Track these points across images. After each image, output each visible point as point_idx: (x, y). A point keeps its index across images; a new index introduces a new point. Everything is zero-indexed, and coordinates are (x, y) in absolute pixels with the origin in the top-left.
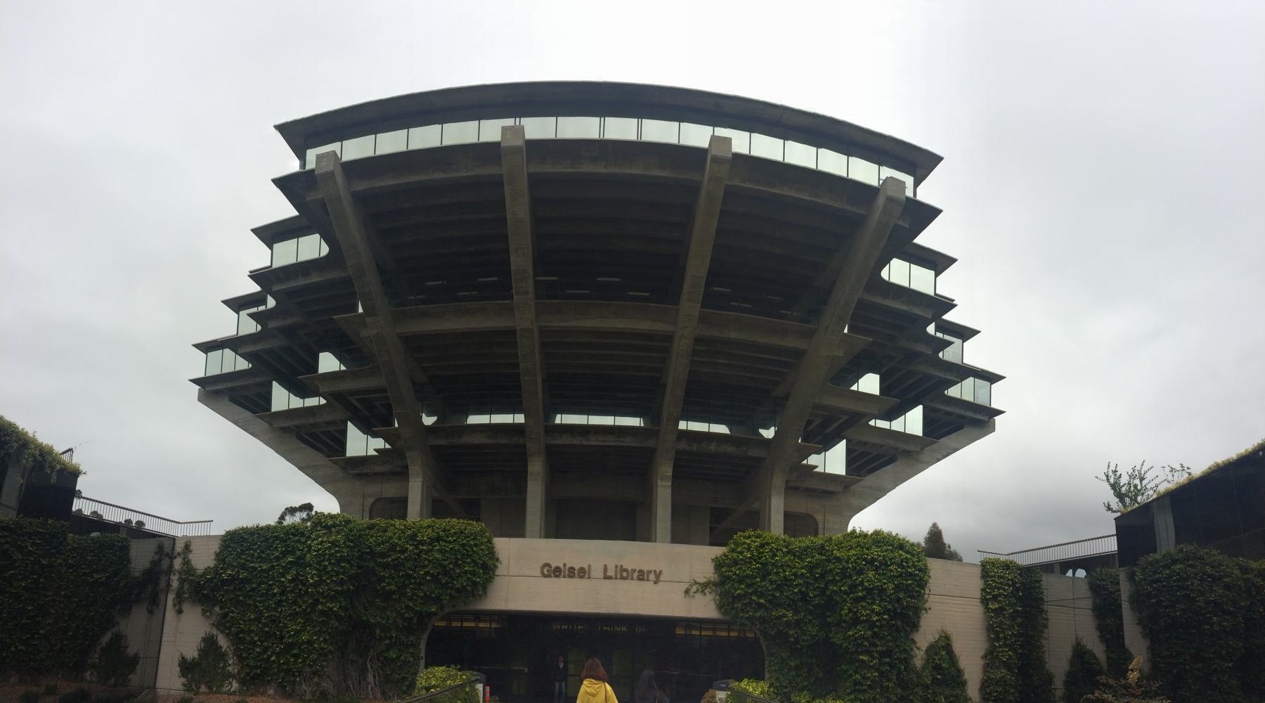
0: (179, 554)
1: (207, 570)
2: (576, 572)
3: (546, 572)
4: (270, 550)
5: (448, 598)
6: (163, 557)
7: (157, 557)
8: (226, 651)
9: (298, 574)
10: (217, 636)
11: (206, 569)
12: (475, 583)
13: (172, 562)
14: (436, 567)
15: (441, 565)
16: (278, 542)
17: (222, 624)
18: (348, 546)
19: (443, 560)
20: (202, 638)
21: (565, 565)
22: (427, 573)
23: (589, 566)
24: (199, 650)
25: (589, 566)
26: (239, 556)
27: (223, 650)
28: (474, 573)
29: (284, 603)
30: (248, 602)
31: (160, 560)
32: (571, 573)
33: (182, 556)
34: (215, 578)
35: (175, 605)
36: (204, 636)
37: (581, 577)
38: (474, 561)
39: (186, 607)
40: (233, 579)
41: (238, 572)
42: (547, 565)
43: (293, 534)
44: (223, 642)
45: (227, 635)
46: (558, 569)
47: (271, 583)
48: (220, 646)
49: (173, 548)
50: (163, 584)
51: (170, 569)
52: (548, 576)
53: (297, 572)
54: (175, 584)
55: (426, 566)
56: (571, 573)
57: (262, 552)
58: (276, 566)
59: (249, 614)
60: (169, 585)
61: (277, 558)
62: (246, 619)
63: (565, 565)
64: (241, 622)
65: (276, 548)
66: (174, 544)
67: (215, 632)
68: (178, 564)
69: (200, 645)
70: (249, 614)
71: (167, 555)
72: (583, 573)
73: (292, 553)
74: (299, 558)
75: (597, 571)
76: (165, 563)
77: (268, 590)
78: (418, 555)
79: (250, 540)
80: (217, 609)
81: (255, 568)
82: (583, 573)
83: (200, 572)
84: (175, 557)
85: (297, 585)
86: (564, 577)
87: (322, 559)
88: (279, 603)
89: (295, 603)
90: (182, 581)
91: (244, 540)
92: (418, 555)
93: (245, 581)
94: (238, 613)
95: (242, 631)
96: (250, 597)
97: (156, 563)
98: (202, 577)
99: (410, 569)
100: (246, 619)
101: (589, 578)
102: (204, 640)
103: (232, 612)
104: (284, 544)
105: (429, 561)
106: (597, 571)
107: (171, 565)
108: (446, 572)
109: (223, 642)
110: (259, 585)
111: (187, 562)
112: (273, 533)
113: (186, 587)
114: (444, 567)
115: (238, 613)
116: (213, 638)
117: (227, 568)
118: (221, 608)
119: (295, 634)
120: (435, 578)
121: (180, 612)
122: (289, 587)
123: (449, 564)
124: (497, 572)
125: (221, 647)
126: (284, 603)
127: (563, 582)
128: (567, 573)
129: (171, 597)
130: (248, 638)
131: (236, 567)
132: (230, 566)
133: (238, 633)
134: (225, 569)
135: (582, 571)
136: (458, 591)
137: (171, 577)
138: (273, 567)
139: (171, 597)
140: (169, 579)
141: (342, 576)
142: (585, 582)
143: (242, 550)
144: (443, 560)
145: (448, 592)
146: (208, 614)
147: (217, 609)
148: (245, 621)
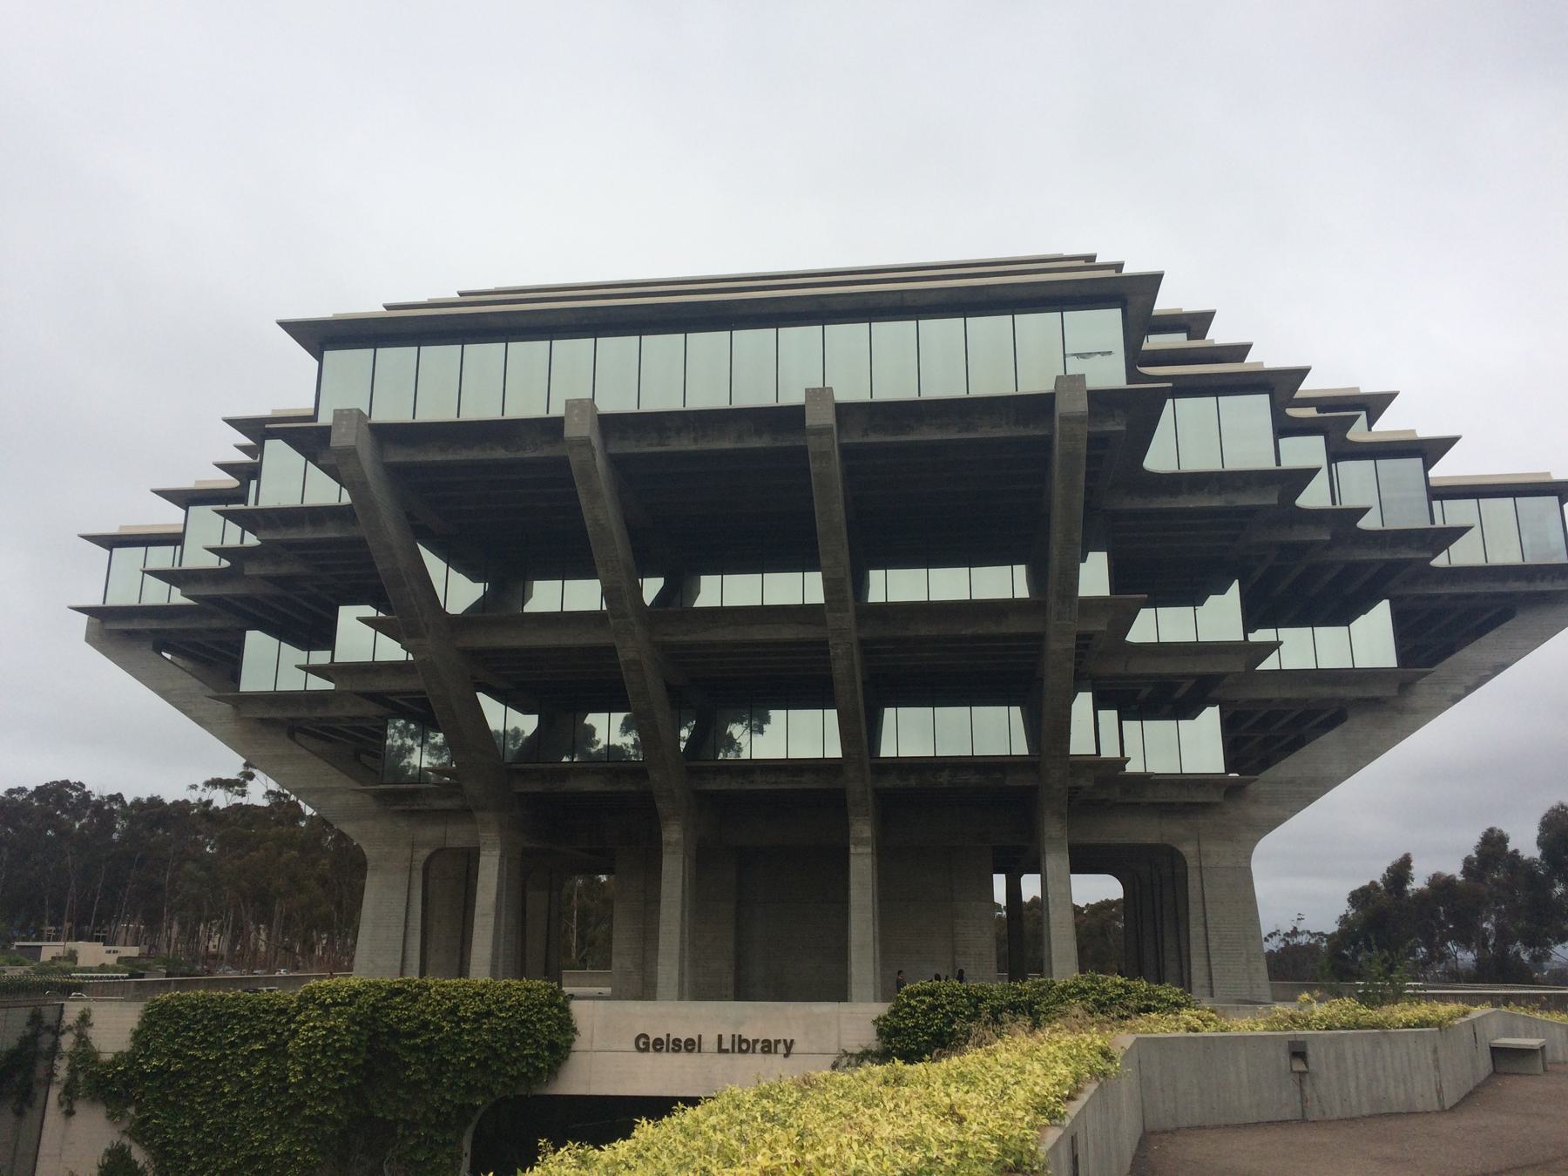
0: (70, 1028)
1: (119, 1057)
2: (682, 1045)
3: (642, 1046)
4: (221, 1031)
5: (499, 1088)
6: (42, 1031)
7: (28, 1031)
8: (143, 1166)
9: (269, 1067)
10: (130, 1147)
11: (116, 1055)
12: (539, 1071)
13: (57, 1039)
14: (484, 1051)
15: (490, 1047)
16: (235, 1021)
17: (140, 1132)
18: (352, 1032)
19: (493, 1042)
20: (106, 1150)
21: (668, 1035)
22: (472, 1059)
23: (700, 1037)
24: (100, 1167)
25: (700, 1037)
26: (171, 1038)
27: (139, 1166)
28: (536, 1056)
29: (242, 1105)
30: (181, 1103)
31: (35, 1036)
32: (677, 1046)
33: (76, 1032)
34: (131, 1068)
35: (61, 1104)
36: (110, 1148)
37: (690, 1051)
38: (536, 1042)
39: (80, 1107)
40: (160, 1071)
41: (169, 1064)
42: (645, 1036)
43: (265, 1011)
44: (139, 1155)
45: (147, 1148)
46: (658, 1041)
47: (220, 1078)
48: (135, 1160)
49: (61, 1018)
50: (40, 1071)
51: (55, 1049)
52: (646, 1050)
53: (268, 1064)
54: (62, 1070)
55: (471, 1049)
56: (677, 1046)
57: (211, 1034)
58: (230, 1055)
59: (182, 1120)
60: (51, 1074)
61: (232, 1045)
62: (177, 1126)
63: (668, 1035)
64: (169, 1130)
65: (232, 1028)
66: (62, 1012)
67: (127, 1141)
68: (67, 1042)
69: (103, 1160)
70: (182, 1120)
71: (48, 1028)
72: (692, 1046)
73: (262, 1035)
74: (274, 1045)
75: (710, 1042)
76: (45, 1041)
77: (214, 1088)
78: (459, 1034)
79: (190, 1017)
80: (132, 1110)
81: (195, 1058)
82: (692, 1046)
83: (107, 1057)
84: (63, 1033)
85: (267, 1081)
86: (667, 1051)
87: (312, 1050)
88: (233, 1106)
89: (262, 1103)
90: (72, 1070)
91: (181, 1015)
92: (459, 1034)
93: (181, 1074)
94: (164, 1118)
95: (170, 1142)
96: (185, 1096)
97: (28, 1042)
98: (109, 1067)
99: (448, 1053)
100: (177, 1126)
101: (699, 1051)
102: (109, 1153)
103: (157, 1117)
104: (248, 1024)
105: (474, 1043)
106: (710, 1042)
107: (55, 1046)
108: (498, 1056)
109: (139, 1155)
110: (201, 1080)
111: (83, 1040)
112: (228, 1007)
113: (81, 1078)
114: (495, 1050)
115: (164, 1118)
116: (124, 1150)
117: (151, 1056)
118: (138, 1111)
119: (260, 1145)
120: (483, 1065)
121: (70, 1113)
122: (256, 1084)
123: (501, 1046)
124: (575, 1046)
125: (136, 1163)
126: (242, 1105)
127: (666, 1058)
128: (671, 1046)
129: (54, 1093)
130: (179, 1152)
131: (166, 1055)
132: (156, 1053)
133: (164, 1145)
134: (148, 1058)
135: (690, 1042)
136: (512, 1077)
137: (55, 1062)
138: (225, 1056)
139: (54, 1093)
140: (53, 1065)
141: (341, 1072)
142: (694, 1057)
143: (176, 1030)
144: (493, 1042)
145: (500, 1080)
146: (117, 1119)
147: (132, 1110)
148: (174, 1129)
